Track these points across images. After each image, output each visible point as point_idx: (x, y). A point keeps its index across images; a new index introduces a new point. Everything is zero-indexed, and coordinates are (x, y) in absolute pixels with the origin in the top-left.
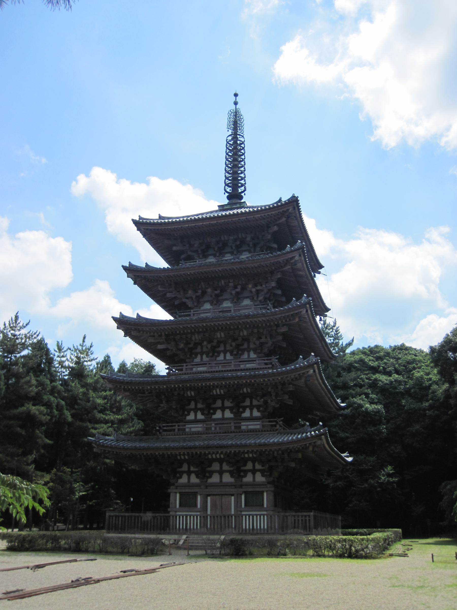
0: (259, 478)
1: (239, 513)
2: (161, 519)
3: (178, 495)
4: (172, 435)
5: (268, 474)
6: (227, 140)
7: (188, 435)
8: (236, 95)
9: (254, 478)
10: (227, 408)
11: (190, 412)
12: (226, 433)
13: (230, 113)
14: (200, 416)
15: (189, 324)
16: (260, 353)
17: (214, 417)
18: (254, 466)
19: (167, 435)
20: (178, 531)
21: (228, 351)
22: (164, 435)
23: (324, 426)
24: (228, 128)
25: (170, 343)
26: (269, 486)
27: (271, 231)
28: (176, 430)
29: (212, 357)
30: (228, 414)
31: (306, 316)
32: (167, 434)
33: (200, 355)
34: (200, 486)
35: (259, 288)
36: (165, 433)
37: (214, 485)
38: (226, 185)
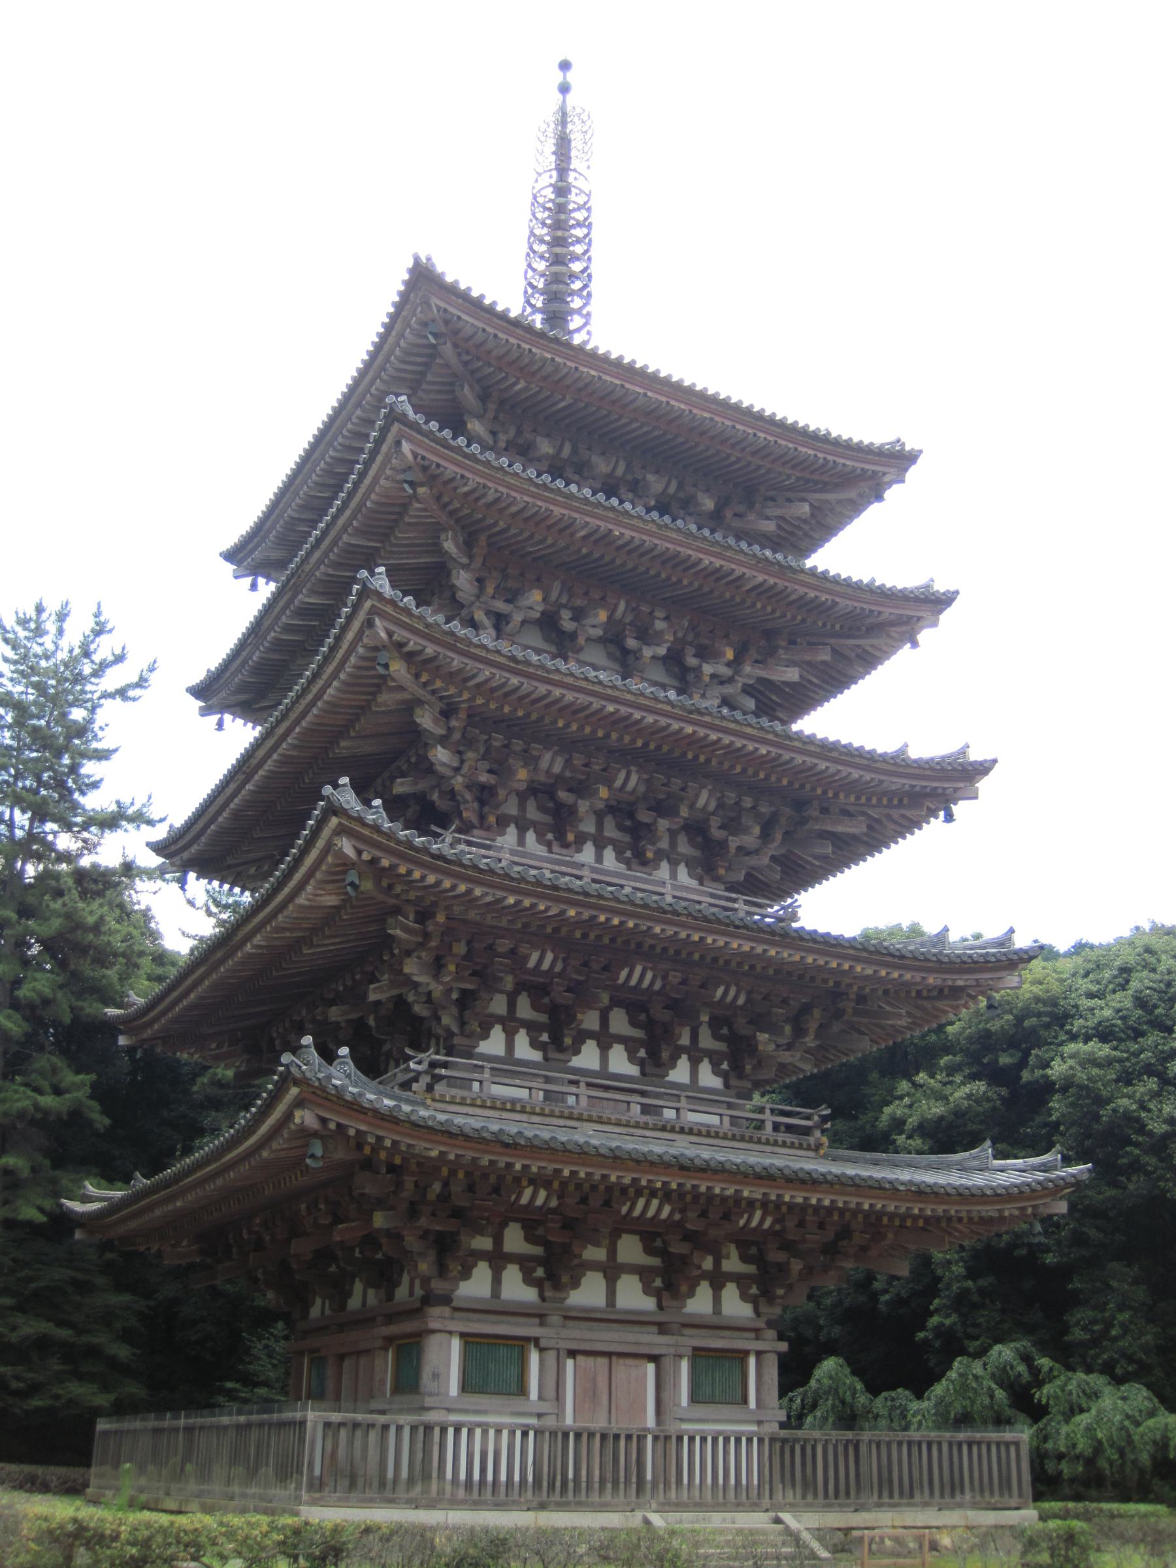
0: (735, 1306)
3: (456, 1344)
7: (533, 1113)
8: (565, 66)
9: (717, 1300)
11: (493, 1027)
14: (524, 1049)
20: (461, 1493)
21: (612, 842)
27: (778, 512)
30: (620, 1063)
37: (587, 1317)
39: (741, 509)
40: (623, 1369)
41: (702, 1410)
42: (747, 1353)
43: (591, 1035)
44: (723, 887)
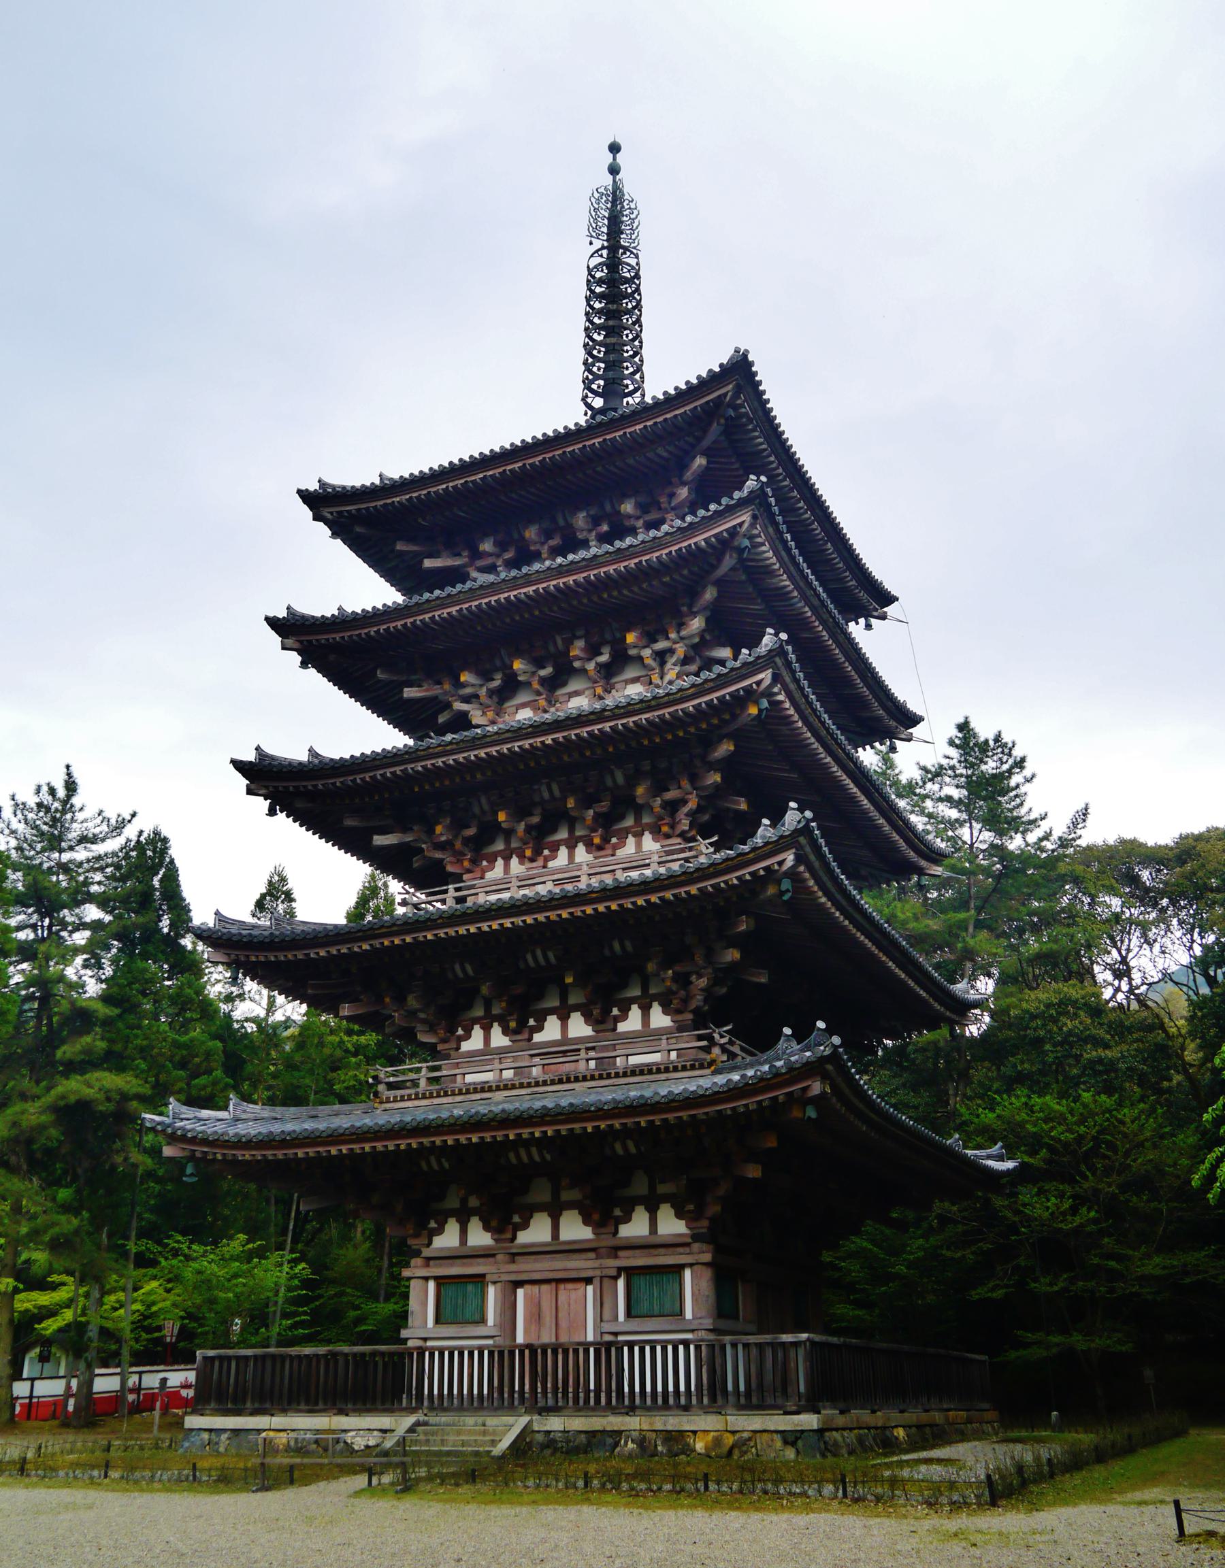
0: (671, 1225)
1: (608, 1338)
2: (347, 1362)
3: (432, 1285)
4: (410, 1099)
5: (691, 1207)
6: (588, 267)
8: (614, 148)
10: (576, 1008)
12: (560, 1082)
13: (597, 195)
14: (499, 1039)
15: (438, 755)
16: (668, 836)
17: (538, 1038)
19: (395, 1101)
22: (388, 1101)
23: (830, 1031)
24: (592, 236)
25: (411, 829)
26: (696, 1246)
28: (423, 1083)
29: (532, 860)
30: (579, 1027)
31: (781, 697)
32: (395, 1097)
33: (503, 858)
34: (493, 1255)
35: (661, 645)
36: (391, 1094)
38: (587, 384)
39: (667, 491)
40: (567, 1294)
41: (634, 1325)
42: (681, 1268)
44: (679, 840)
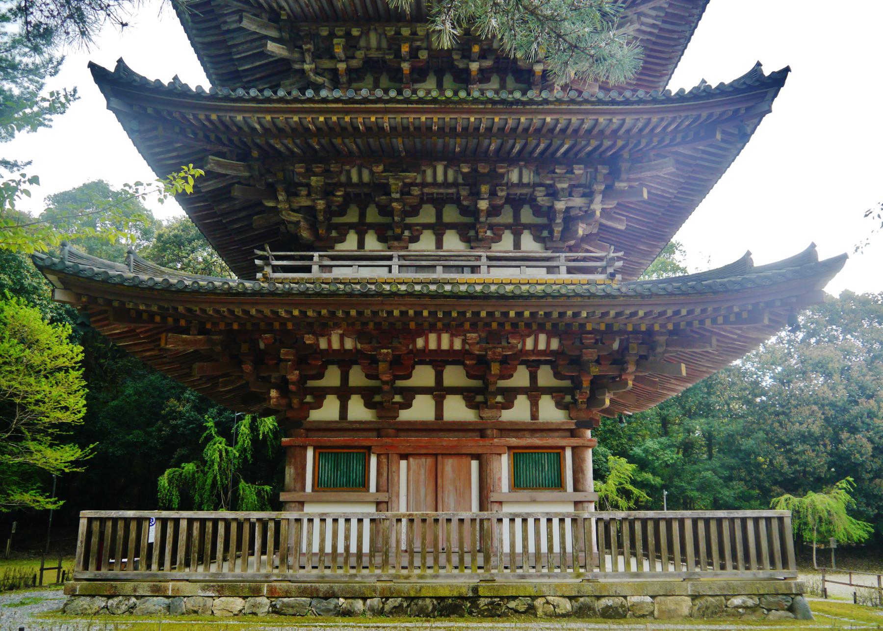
14: (372, 243)
18: (533, 378)
40: (449, 465)
42: (563, 448)
43: (426, 226)
